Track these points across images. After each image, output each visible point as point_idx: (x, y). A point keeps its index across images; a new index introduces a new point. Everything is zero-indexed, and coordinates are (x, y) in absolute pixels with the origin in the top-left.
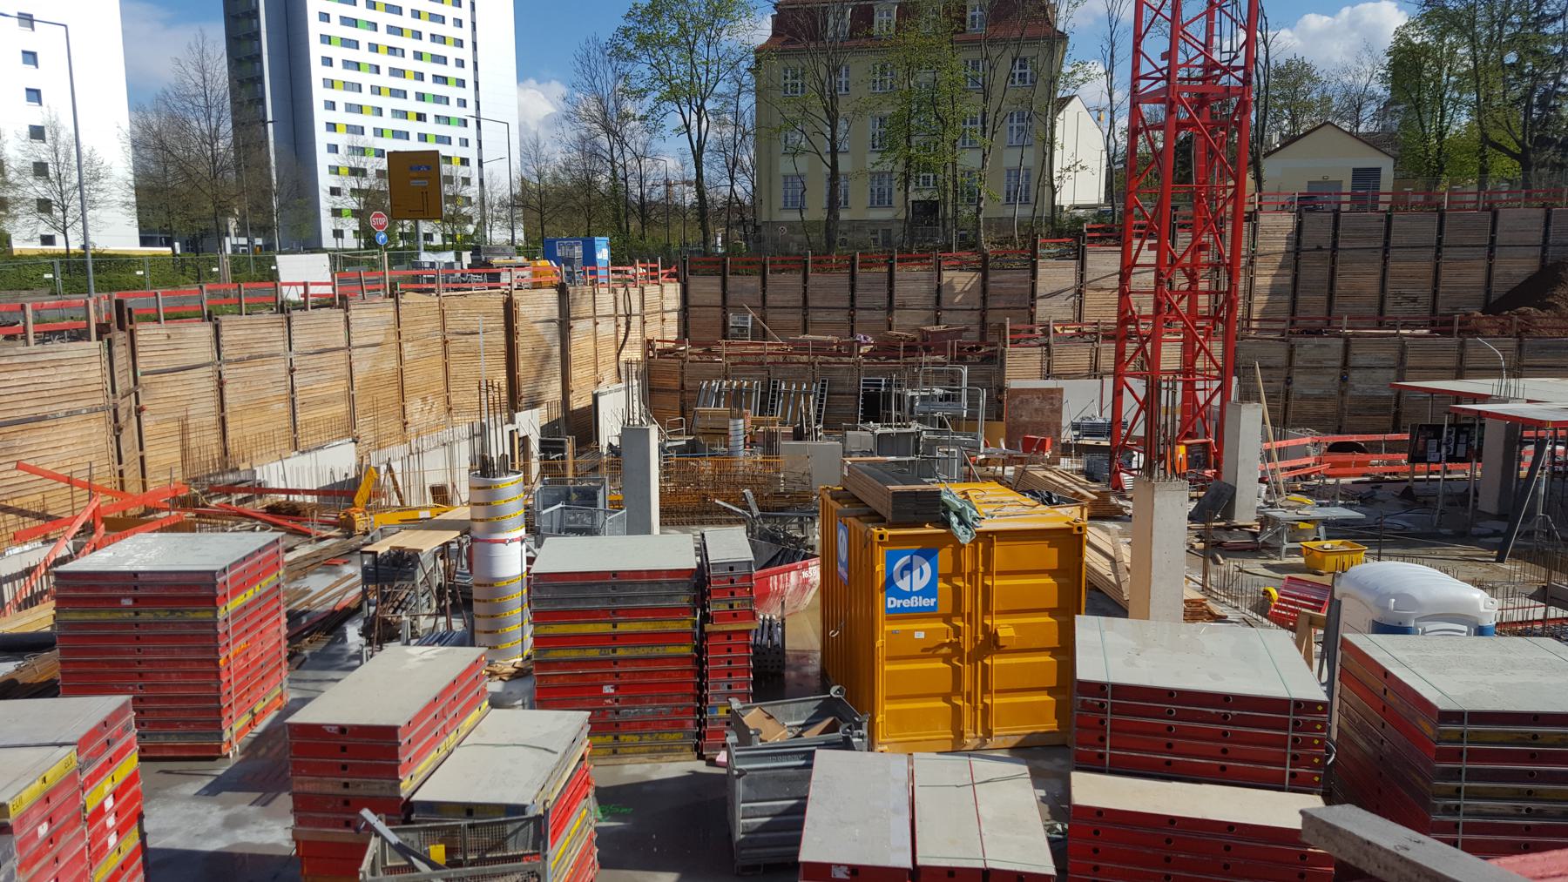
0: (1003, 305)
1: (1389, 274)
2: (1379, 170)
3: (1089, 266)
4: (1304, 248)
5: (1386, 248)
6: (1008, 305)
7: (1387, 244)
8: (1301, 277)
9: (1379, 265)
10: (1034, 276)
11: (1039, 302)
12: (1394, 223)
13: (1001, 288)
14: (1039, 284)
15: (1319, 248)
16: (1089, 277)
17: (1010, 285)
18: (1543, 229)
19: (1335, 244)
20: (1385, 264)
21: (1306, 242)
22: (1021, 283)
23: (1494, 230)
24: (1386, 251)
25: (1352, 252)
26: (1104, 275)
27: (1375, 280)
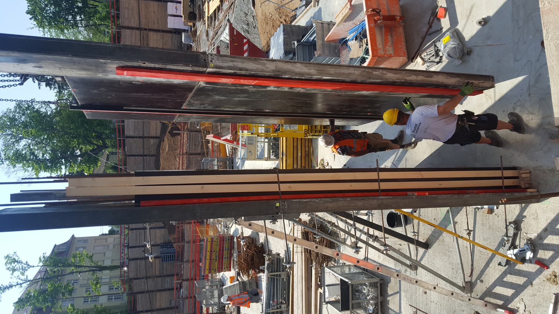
27: (158, 231)
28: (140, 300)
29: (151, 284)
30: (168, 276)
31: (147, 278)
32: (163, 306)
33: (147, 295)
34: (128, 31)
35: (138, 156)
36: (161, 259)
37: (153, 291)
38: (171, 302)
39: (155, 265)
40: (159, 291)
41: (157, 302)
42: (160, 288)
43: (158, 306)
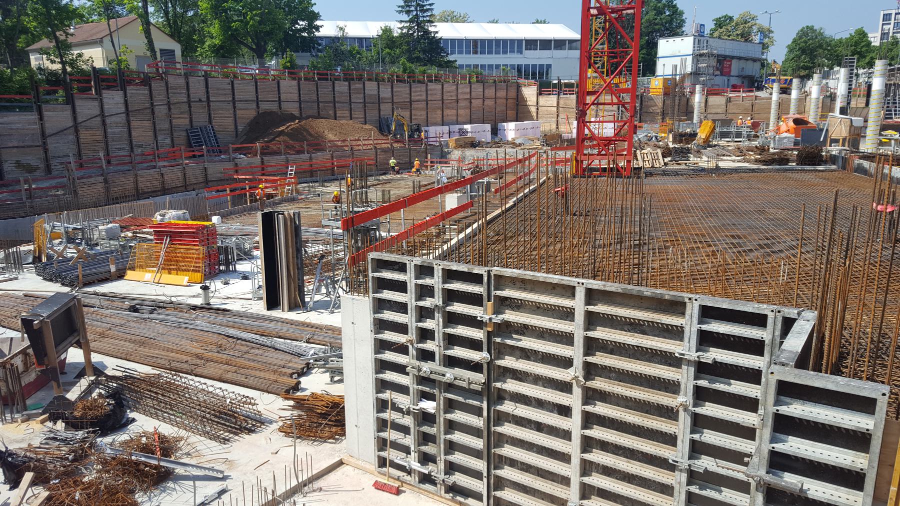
0: (16, 144)
1: (237, 118)
2: (174, 51)
3: (78, 110)
4: (193, 100)
5: (234, 101)
6: (21, 144)
7: (234, 98)
8: (194, 120)
9: (232, 111)
10: (41, 118)
11: (49, 140)
12: (235, 86)
13: (12, 129)
14: (47, 125)
15: (200, 100)
16: (80, 120)
17: (20, 126)
18: (296, 91)
19: (208, 98)
20: (235, 111)
21: (193, 98)
22: (29, 124)
23: (279, 93)
24: (234, 104)
25: (217, 104)
26: (89, 117)
27: (231, 120)
28: (141, 92)
29: (161, 111)
30: (172, 139)
31: (169, 104)
32: (134, 134)
33: (148, 105)
34: (408, 90)
35: (318, 95)
36: (189, 127)
37: (153, 113)
38: (141, 146)
39: (182, 118)
40: (154, 123)
41: (139, 123)
42: (157, 127)
43: (134, 124)
